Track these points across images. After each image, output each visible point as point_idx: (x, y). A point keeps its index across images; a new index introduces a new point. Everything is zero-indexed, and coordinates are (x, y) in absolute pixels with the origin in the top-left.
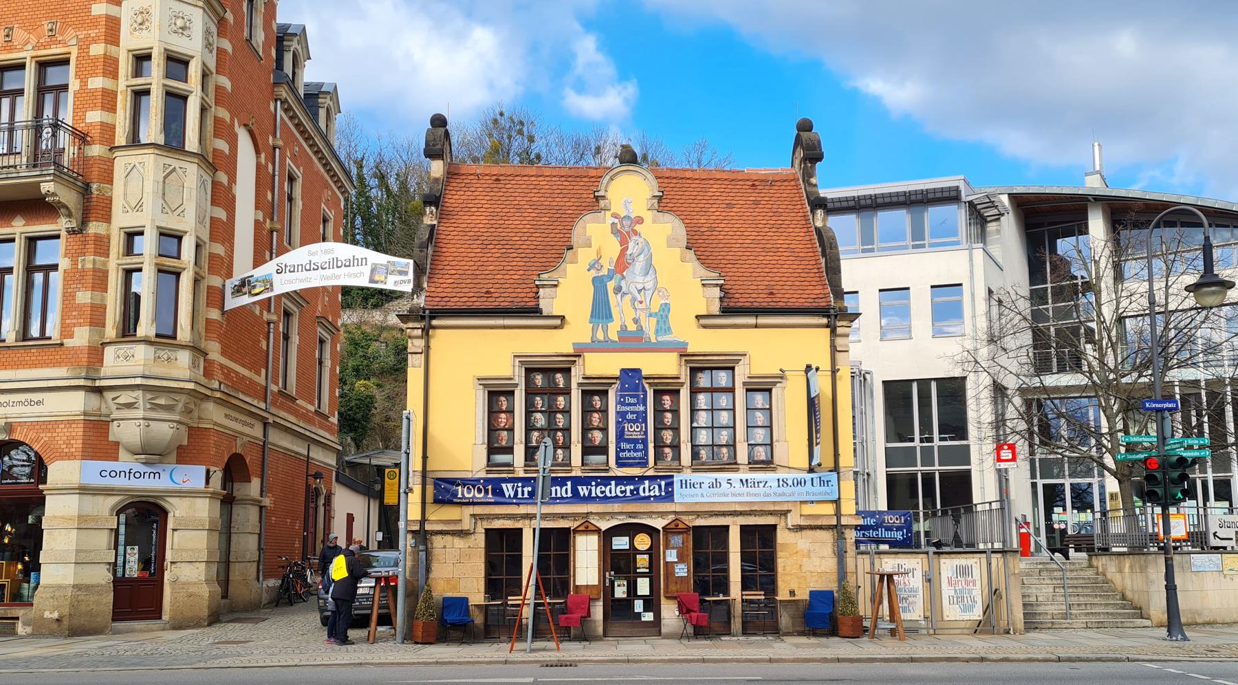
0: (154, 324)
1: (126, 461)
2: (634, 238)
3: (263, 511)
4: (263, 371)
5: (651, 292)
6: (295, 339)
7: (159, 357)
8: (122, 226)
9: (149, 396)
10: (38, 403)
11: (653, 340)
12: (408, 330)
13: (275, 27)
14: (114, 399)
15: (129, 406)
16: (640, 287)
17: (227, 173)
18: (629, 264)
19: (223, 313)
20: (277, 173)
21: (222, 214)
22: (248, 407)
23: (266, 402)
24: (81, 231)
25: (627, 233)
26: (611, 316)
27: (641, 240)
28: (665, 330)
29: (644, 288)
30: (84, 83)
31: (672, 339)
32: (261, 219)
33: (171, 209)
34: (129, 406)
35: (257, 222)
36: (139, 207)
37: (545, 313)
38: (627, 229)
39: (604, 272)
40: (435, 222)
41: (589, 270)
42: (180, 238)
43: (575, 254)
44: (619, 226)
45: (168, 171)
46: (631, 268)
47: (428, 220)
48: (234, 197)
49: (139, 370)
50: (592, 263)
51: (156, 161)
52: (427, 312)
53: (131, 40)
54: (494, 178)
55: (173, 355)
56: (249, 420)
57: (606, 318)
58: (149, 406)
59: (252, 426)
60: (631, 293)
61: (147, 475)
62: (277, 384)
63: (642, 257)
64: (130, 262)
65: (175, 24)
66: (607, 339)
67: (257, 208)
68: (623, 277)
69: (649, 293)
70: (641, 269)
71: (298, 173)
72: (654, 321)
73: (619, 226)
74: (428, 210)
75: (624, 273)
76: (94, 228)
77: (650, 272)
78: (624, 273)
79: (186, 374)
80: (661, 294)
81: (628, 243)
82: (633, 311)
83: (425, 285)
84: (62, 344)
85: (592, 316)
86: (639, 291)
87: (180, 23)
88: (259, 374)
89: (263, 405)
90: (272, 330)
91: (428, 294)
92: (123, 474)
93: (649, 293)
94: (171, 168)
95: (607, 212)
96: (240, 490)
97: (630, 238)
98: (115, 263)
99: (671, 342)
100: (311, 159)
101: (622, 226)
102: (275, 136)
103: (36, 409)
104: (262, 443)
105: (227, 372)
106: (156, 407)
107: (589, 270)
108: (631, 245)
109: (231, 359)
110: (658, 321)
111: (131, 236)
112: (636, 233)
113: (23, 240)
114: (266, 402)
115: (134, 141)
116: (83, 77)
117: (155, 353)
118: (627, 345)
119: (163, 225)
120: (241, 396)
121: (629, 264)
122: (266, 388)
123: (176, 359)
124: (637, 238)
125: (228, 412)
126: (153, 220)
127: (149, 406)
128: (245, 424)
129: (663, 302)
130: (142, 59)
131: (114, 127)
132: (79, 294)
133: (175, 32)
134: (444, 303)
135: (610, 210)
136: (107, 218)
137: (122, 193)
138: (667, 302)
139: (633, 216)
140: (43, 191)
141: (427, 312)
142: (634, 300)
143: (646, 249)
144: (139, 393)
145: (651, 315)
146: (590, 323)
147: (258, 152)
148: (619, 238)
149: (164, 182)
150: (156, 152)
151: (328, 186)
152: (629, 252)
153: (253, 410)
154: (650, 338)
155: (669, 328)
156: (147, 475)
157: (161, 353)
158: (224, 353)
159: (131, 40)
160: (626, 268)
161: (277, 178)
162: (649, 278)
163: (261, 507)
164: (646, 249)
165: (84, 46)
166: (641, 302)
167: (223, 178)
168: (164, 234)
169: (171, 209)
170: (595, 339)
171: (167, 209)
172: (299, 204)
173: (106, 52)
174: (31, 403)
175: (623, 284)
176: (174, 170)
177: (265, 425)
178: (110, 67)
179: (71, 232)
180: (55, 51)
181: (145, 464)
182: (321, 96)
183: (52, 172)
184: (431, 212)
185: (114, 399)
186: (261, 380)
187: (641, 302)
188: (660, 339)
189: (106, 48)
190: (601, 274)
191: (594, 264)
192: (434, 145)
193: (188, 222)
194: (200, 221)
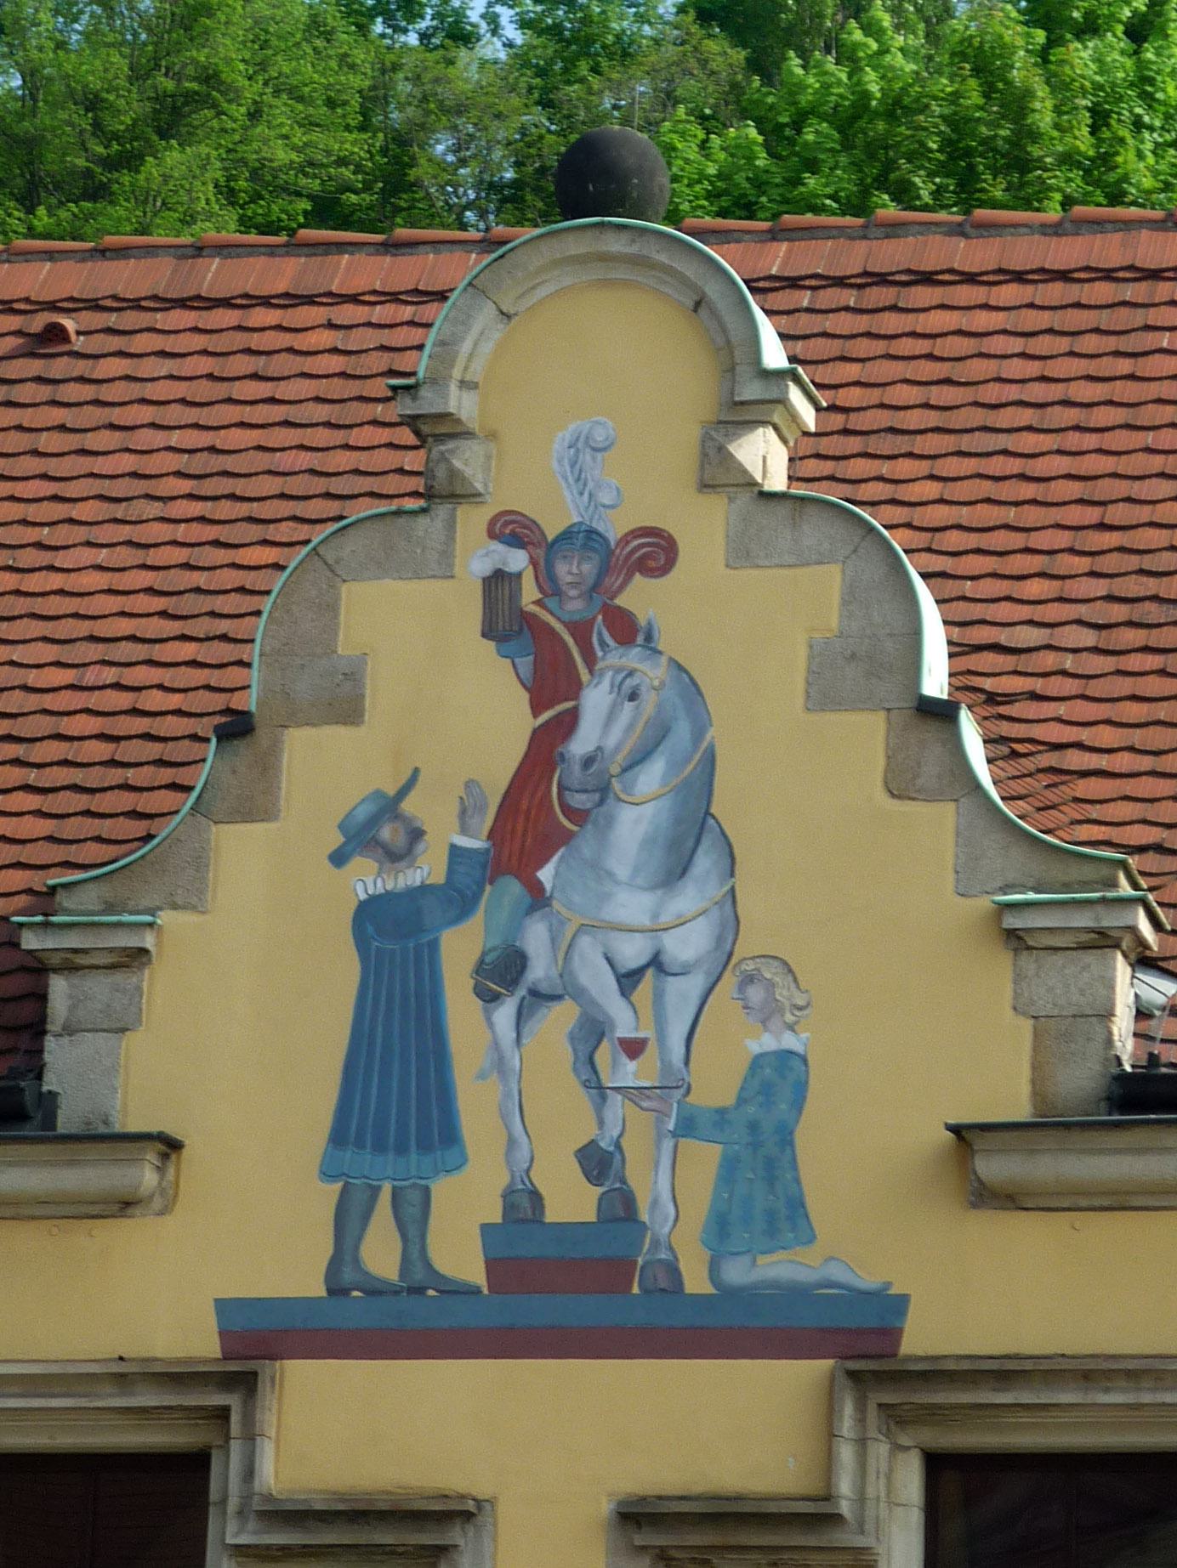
2: (614, 658)
5: (694, 985)
11: (696, 1281)
16: (632, 952)
18: (579, 816)
25: (581, 631)
26: (449, 1135)
27: (652, 673)
28: (771, 1216)
29: (656, 962)
31: (804, 1276)
37: (66, 1121)
38: (575, 607)
39: (428, 868)
41: (339, 858)
43: (268, 767)
44: (529, 593)
46: (586, 844)
50: (362, 814)
54: (38, 323)
57: (425, 1146)
60: (579, 994)
63: (652, 777)
66: (419, 1275)
68: (538, 898)
69: (683, 993)
70: (648, 842)
72: (704, 1158)
73: (529, 593)
75: (546, 875)
77: (704, 862)
78: (546, 875)
80: (755, 994)
81: (575, 689)
82: (582, 1099)
85: (338, 1138)
86: (628, 981)
93: (683, 993)
95: (463, 512)
97: (590, 660)
99: (797, 1293)
101: (550, 587)
107: (339, 858)
108: (596, 699)
110: (729, 1170)
112: (626, 629)
118: (539, 1309)
121: (579, 816)
124: (632, 657)
129: (767, 1042)
135: (473, 497)
138: (790, 1042)
139: (614, 528)
142: (592, 1031)
143: (682, 730)
145: (688, 1127)
146: (327, 1175)
148: (526, 663)
152: (580, 745)
154: (673, 1270)
155: (797, 1206)
160: (549, 842)
162: (688, 899)
164: (682, 730)
166: (633, 1048)
170: (348, 1276)
175: (536, 939)
187: (633, 1048)
188: (736, 1273)
190: (412, 877)
191: (374, 821)
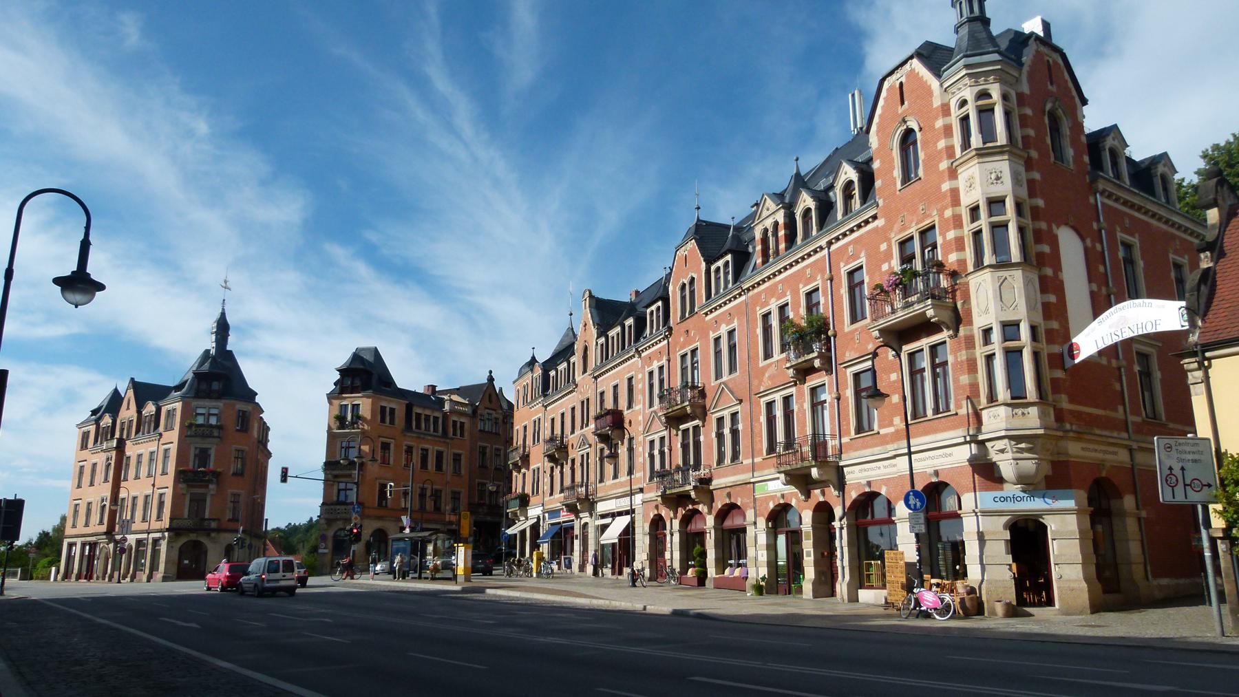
0: (1009, 390)
1: (1012, 489)
3: (1142, 521)
4: (1121, 409)
6: (1157, 375)
7: (1016, 414)
8: (979, 326)
9: (1013, 443)
10: (950, 455)
12: (1185, 365)
13: (1084, 139)
14: (992, 447)
15: (1002, 451)
17: (1051, 266)
19: (1065, 370)
20: (1106, 249)
21: (1052, 298)
22: (1104, 439)
23: (1127, 431)
24: (956, 336)
30: (944, 238)
32: (1095, 287)
33: (1007, 307)
34: (1002, 451)
35: (1092, 294)
36: (987, 311)
40: (1211, 265)
42: (1018, 325)
45: (1001, 281)
47: (1205, 262)
48: (1062, 282)
49: (1003, 426)
51: (992, 277)
52: (1199, 347)
53: (967, 199)
55: (1025, 411)
56: (1111, 449)
58: (1015, 450)
59: (1115, 453)
61: (1025, 498)
62: (1139, 414)
64: (988, 350)
65: (991, 178)
67: (1090, 280)
71: (1135, 240)
74: (1202, 256)
76: (962, 331)
79: (1037, 423)
83: (1200, 323)
84: (957, 414)
87: (993, 176)
88: (1116, 410)
89: (1125, 435)
90: (1123, 374)
91: (1202, 330)
92: (1009, 499)
94: (1003, 278)
96: (1114, 504)
98: (980, 352)
100: (1147, 224)
102: (1098, 220)
103: (949, 459)
104: (1130, 466)
105: (1078, 416)
106: (1021, 450)
109: (1080, 403)
111: (987, 332)
113: (906, 356)
114: (1127, 431)
115: (979, 265)
116: (943, 234)
117: (1013, 411)
119: (1004, 319)
120: (610, 493)
122: (1126, 421)
123: (1029, 413)
125: (1084, 445)
126: (996, 318)
127: (1015, 450)
128: (1105, 452)
130: (974, 211)
131: (965, 260)
132: (961, 378)
133: (992, 183)
134: (1216, 336)
136: (970, 323)
137: (976, 303)
140: (928, 316)
141: (1199, 347)
144: (1006, 441)
147: (1083, 238)
149: (1000, 289)
150: (992, 270)
151: (1173, 237)
153: (1111, 440)
156: (1025, 498)
157: (1016, 410)
158: (1071, 401)
159: (967, 199)
161: (1106, 253)
163: (1139, 519)
165: (941, 215)
167: (1049, 272)
168: (1006, 325)
169: (1007, 307)
171: (1005, 308)
172: (1141, 264)
173: (953, 212)
174: (946, 455)
176: (1006, 278)
177: (1131, 450)
178: (957, 222)
179: (950, 337)
180: (926, 223)
181: (1024, 491)
182: (1153, 167)
183: (930, 303)
184: (1206, 257)
185: (992, 447)
186: (1120, 414)
189: (953, 210)
192: (1206, 197)
193: (1020, 311)
194: (1030, 307)
